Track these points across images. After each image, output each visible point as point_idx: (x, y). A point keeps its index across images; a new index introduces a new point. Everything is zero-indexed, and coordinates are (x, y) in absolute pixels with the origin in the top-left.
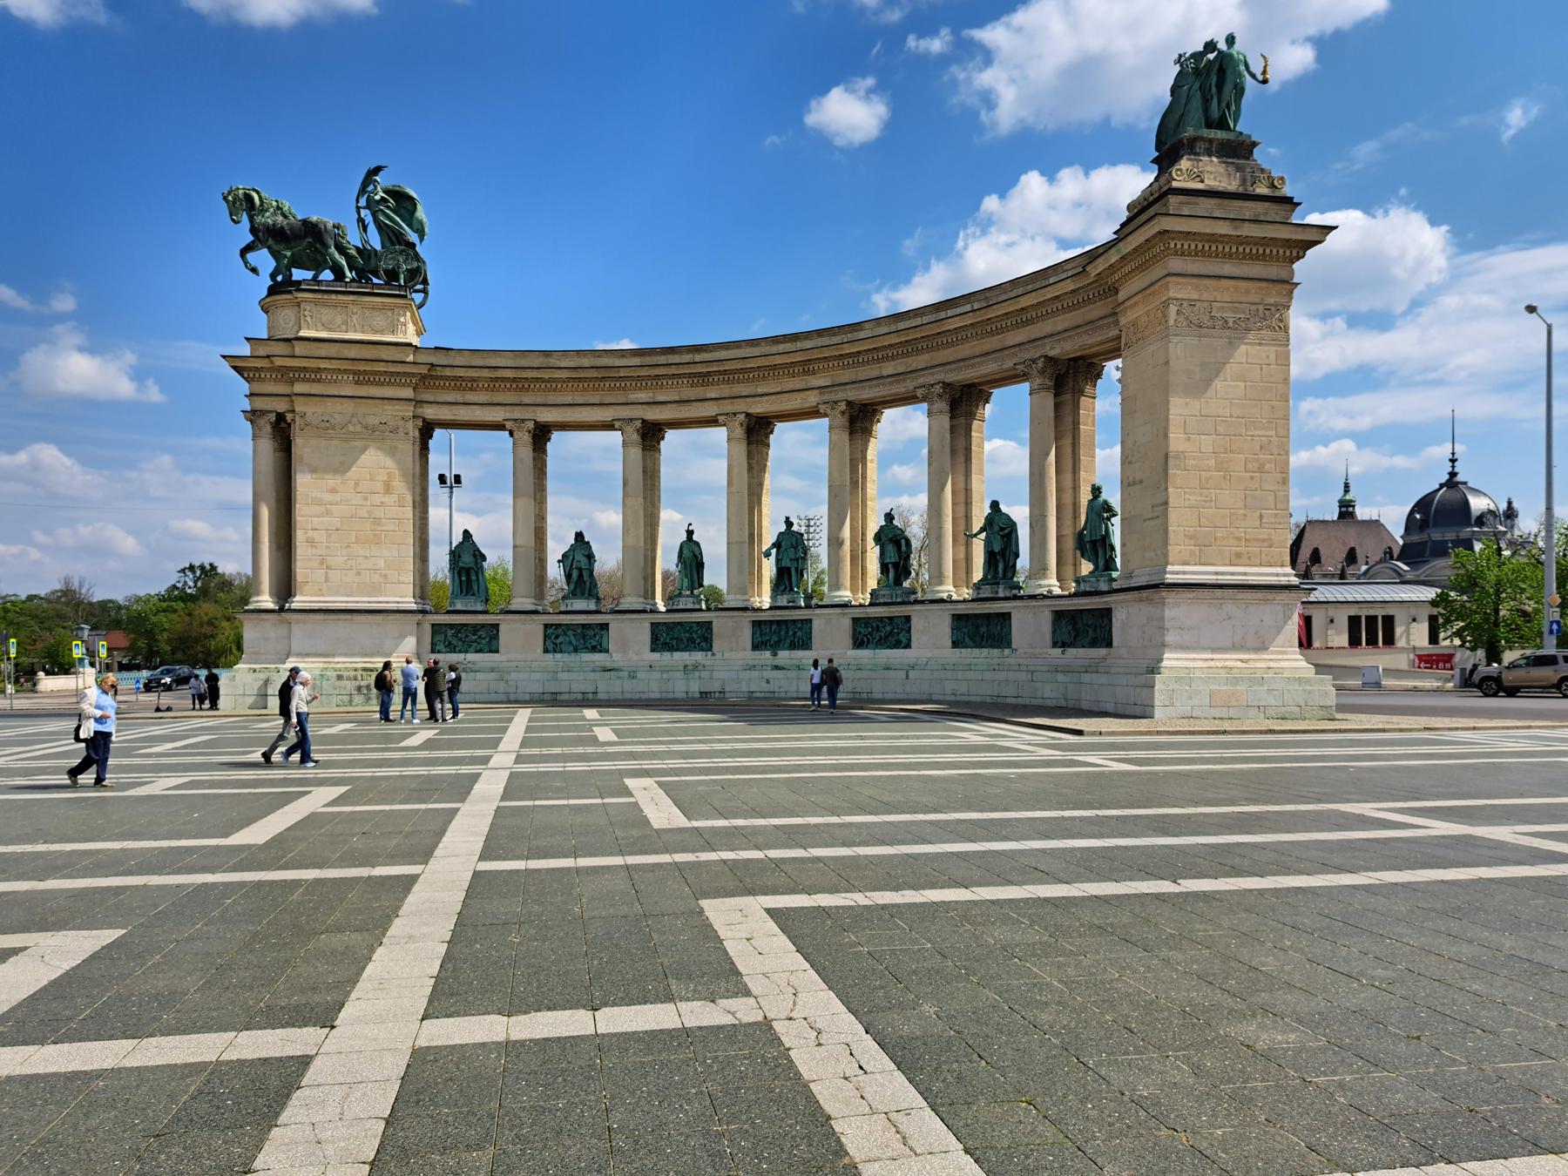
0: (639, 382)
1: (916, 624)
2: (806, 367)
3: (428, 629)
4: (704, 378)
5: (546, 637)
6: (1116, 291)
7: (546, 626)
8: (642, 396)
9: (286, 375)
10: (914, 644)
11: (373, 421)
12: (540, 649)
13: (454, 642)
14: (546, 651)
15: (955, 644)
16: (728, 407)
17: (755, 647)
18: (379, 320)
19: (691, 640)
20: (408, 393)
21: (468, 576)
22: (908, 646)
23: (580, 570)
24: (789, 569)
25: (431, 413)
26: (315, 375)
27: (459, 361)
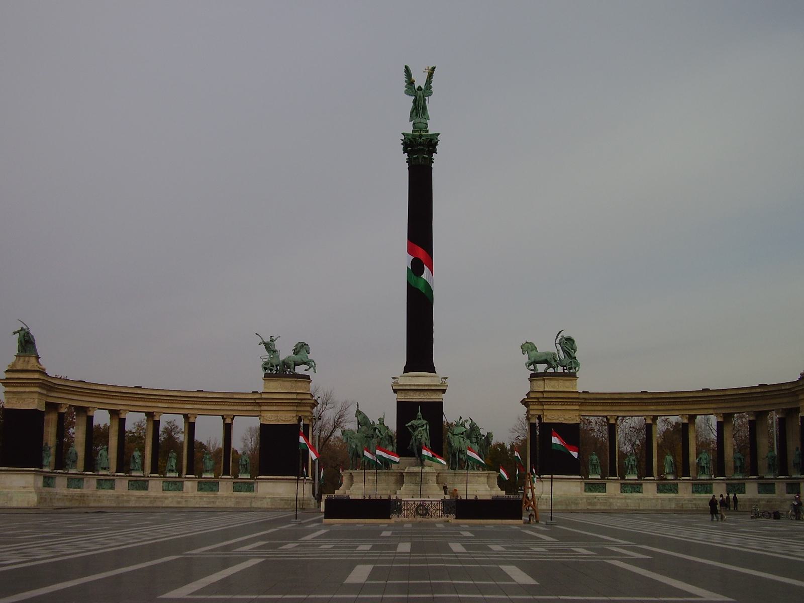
0: (651, 404)
1: (747, 486)
2: (709, 402)
3: (583, 484)
4: (674, 403)
6: (797, 395)
7: (621, 484)
8: (653, 408)
9: (541, 404)
10: (746, 492)
12: (619, 492)
13: (592, 488)
14: (621, 492)
15: (759, 492)
16: (682, 413)
17: (693, 492)
18: (568, 383)
19: (672, 490)
21: (595, 467)
22: (744, 493)
23: (632, 465)
24: (704, 466)
25: (583, 413)
26: (550, 403)
27: (592, 396)
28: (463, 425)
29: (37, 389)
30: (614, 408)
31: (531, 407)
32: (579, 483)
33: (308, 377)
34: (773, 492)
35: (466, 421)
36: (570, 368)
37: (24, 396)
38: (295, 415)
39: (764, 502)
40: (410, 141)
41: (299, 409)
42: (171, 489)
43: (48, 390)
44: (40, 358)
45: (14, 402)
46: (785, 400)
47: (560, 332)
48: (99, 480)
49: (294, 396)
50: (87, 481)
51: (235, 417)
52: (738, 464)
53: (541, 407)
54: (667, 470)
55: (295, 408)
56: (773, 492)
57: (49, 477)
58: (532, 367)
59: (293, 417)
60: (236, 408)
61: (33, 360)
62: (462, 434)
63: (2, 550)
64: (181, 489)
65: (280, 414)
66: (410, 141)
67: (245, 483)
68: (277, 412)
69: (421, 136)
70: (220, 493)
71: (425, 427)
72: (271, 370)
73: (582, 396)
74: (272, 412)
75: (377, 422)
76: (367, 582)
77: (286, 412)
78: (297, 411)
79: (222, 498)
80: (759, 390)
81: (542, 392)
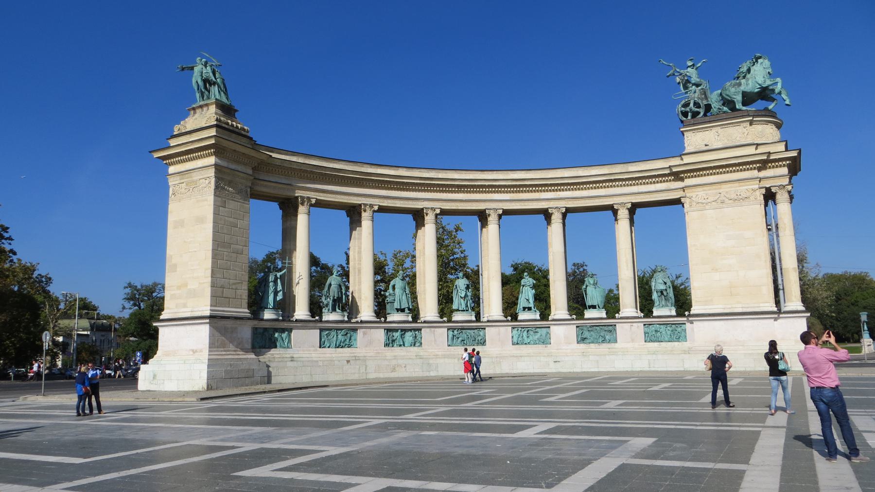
29: (212, 160)
37: (196, 176)
38: (757, 186)
41: (763, 174)
42: (527, 340)
44: (236, 111)
45: (183, 190)
49: (751, 150)
50: (364, 334)
51: (638, 211)
55: (755, 173)
59: (754, 190)
64: (545, 341)
65: (725, 188)
68: (718, 186)
74: (705, 188)
77: (737, 184)
78: (761, 179)
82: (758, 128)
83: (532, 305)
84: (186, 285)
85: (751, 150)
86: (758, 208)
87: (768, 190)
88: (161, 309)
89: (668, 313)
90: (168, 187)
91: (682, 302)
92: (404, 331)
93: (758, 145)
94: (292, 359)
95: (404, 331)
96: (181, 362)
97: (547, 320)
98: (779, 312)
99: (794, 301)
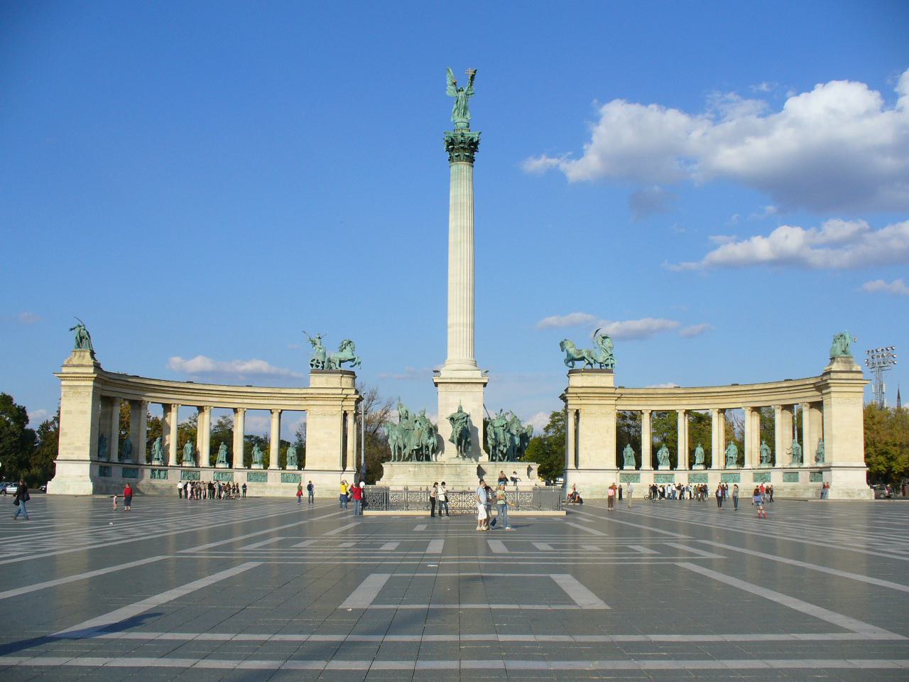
5: (655, 478)
11: (604, 411)
15: (784, 481)
20: (613, 402)
27: (628, 391)
28: (504, 418)
30: (649, 403)
31: (569, 402)
32: (615, 474)
33: (352, 373)
34: (796, 480)
35: (508, 413)
36: (607, 365)
37: (80, 390)
39: (788, 490)
40: (452, 140)
43: (102, 384)
46: (810, 394)
47: (597, 331)
48: (153, 471)
49: (340, 391)
52: (764, 454)
53: (580, 402)
54: (698, 461)
56: (796, 480)
57: (105, 467)
58: (570, 364)
60: (283, 402)
61: (88, 354)
62: (503, 426)
63: (3, 542)
65: (327, 408)
66: (452, 140)
67: (293, 474)
69: (463, 135)
70: (269, 483)
71: (465, 420)
72: (317, 366)
73: (618, 391)
75: (418, 415)
76: (375, 607)
79: (271, 487)
80: (785, 385)
81: (581, 387)
82: (344, 380)
83: (225, 460)
84: (74, 444)
85: (340, 391)
86: (339, 420)
87: (345, 411)
88: (56, 453)
89: (293, 468)
90: (61, 392)
91: (301, 465)
92: (160, 470)
93: (343, 389)
94: (113, 482)
95: (160, 470)
96: (72, 477)
97: (167, 466)
98: (344, 471)
99: (351, 466)
